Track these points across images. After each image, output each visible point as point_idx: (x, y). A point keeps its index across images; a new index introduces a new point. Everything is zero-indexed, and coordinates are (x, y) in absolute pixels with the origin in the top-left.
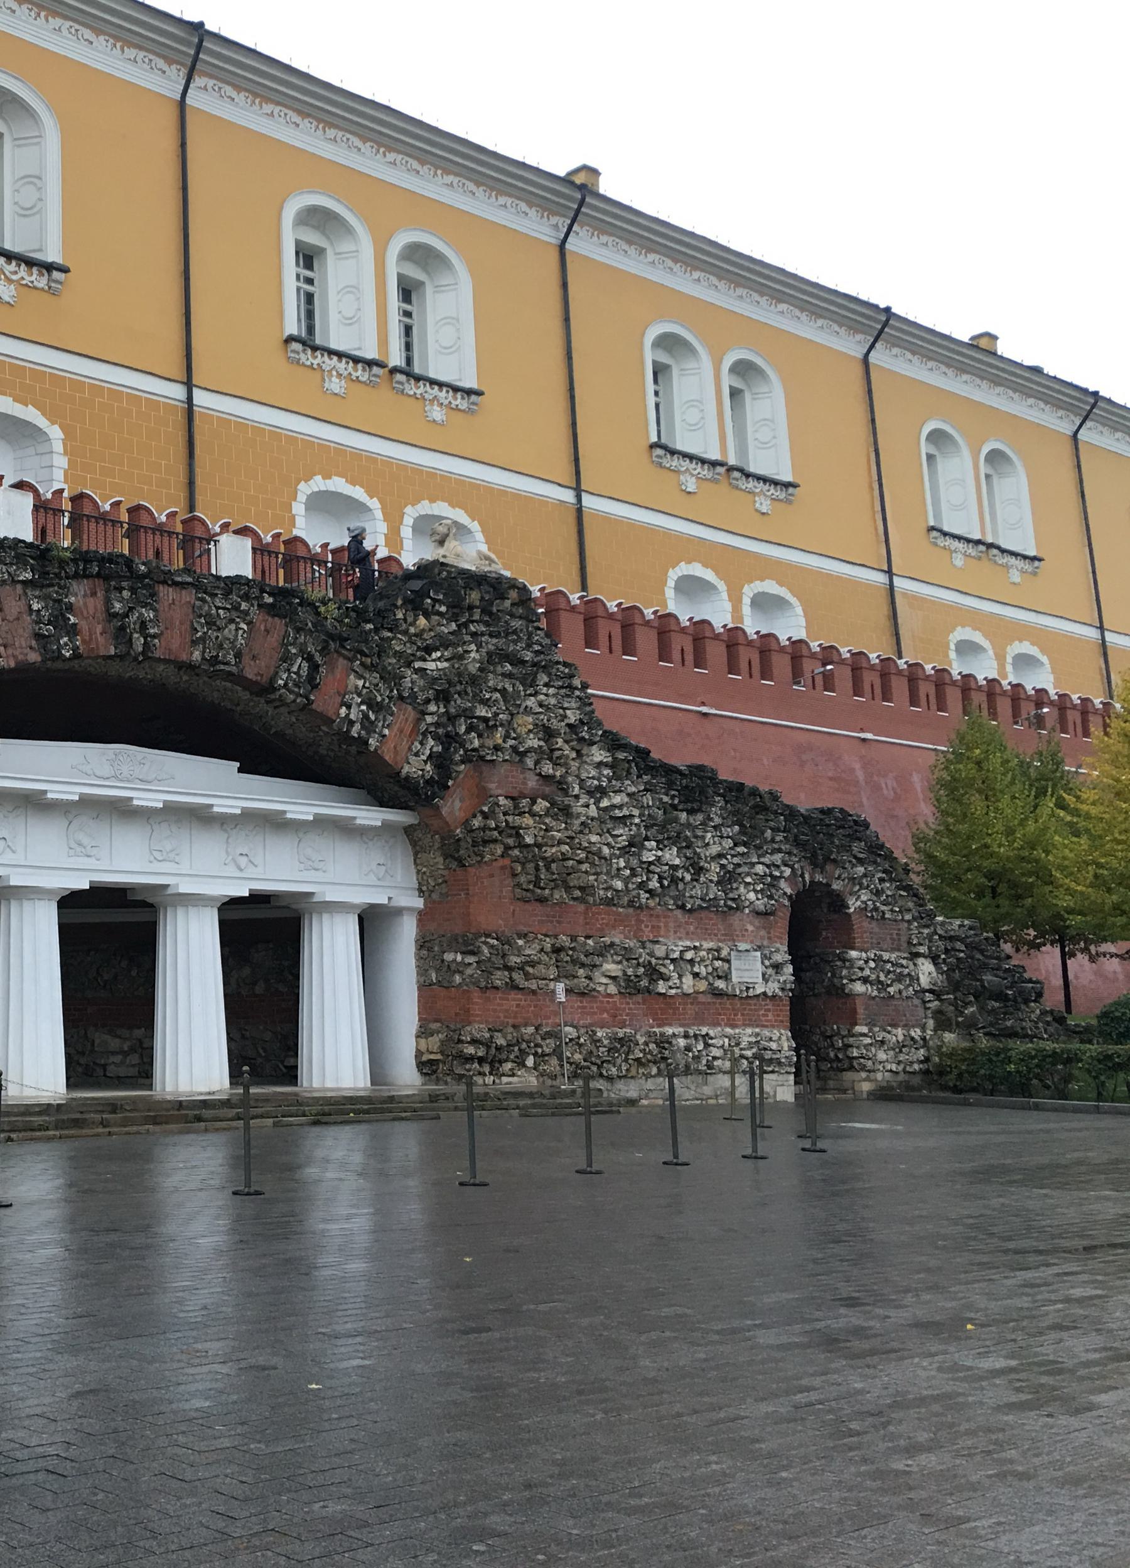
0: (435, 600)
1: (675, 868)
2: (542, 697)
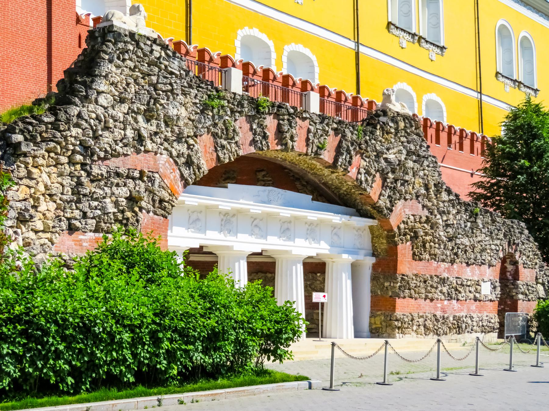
0: (391, 127)
1: (466, 246)
2: (426, 171)
